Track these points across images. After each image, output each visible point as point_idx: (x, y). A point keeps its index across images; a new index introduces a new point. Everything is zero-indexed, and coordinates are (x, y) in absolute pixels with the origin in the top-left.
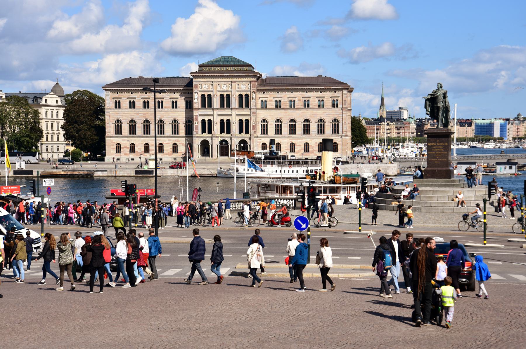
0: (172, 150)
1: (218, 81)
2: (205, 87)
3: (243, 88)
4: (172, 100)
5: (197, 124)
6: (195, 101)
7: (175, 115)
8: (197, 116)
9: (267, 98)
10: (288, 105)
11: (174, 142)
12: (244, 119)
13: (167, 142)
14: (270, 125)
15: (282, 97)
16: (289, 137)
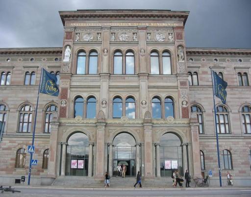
0: (14, 162)
1: (111, 28)
2: (86, 38)
3: (159, 38)
4: (26, 70)
5: (65, 105)
6: (66, 60)
7: (29, 95)
8: (65, 91)
9: (199, 67)
10: (235, 80)
11: (20, 146)
12: (163, 96)
13: (5, 147)
14: (209, 115)
15: (224, 68)
16: (245, 138)
